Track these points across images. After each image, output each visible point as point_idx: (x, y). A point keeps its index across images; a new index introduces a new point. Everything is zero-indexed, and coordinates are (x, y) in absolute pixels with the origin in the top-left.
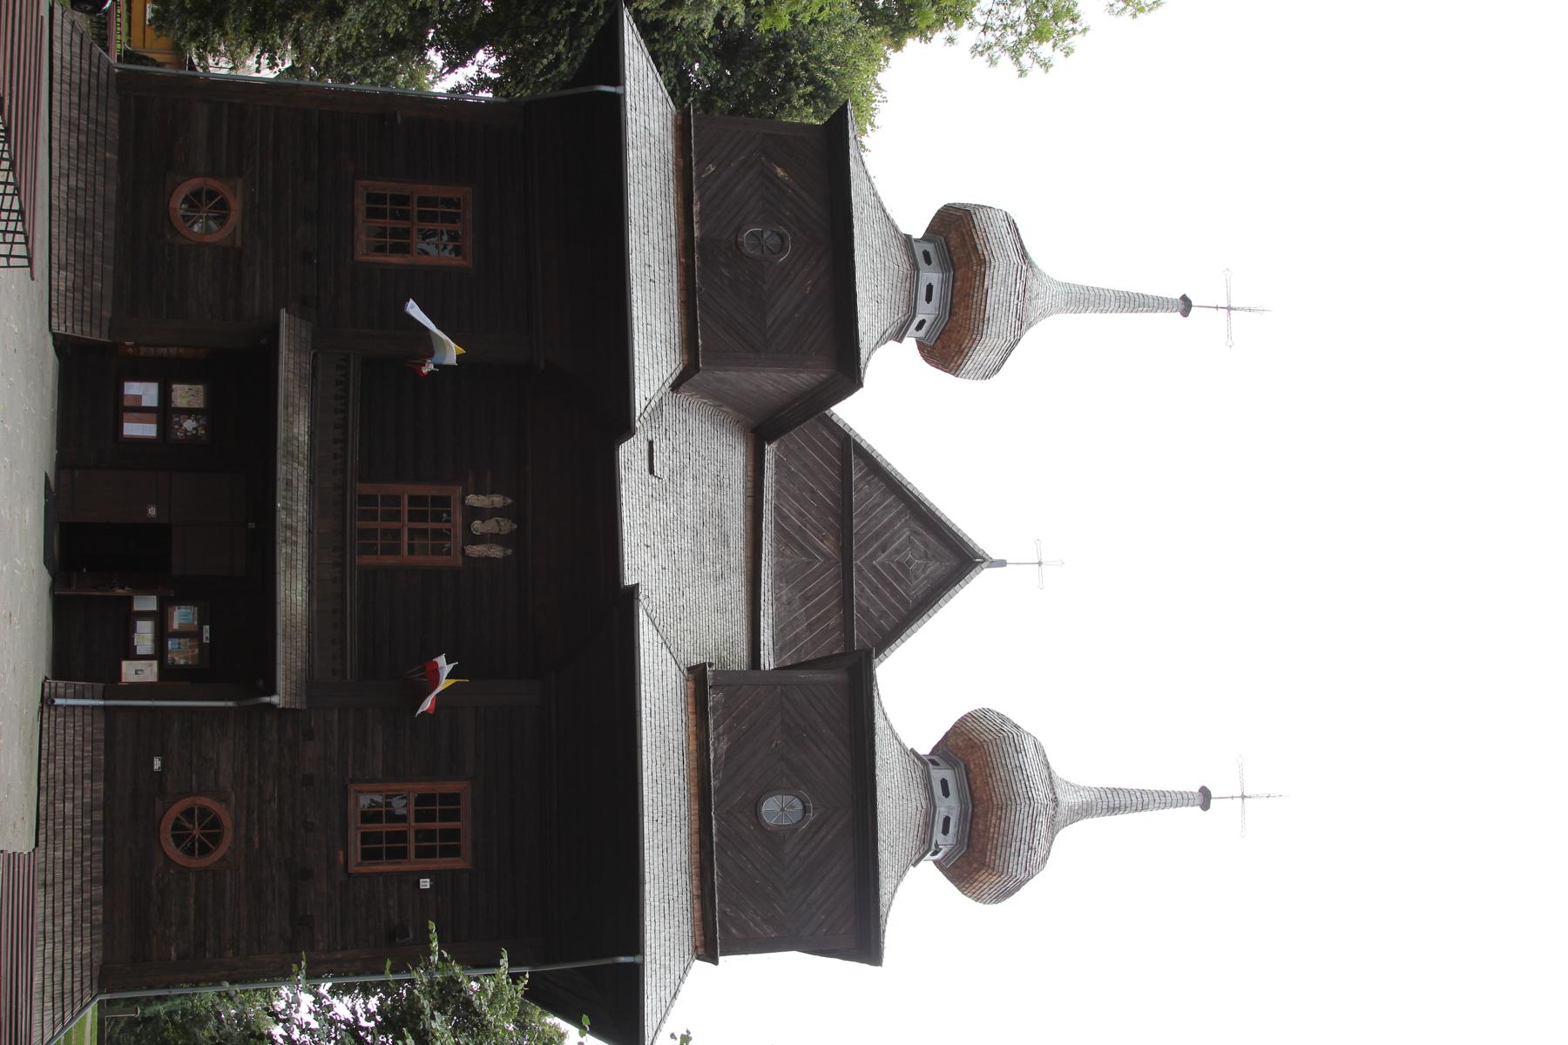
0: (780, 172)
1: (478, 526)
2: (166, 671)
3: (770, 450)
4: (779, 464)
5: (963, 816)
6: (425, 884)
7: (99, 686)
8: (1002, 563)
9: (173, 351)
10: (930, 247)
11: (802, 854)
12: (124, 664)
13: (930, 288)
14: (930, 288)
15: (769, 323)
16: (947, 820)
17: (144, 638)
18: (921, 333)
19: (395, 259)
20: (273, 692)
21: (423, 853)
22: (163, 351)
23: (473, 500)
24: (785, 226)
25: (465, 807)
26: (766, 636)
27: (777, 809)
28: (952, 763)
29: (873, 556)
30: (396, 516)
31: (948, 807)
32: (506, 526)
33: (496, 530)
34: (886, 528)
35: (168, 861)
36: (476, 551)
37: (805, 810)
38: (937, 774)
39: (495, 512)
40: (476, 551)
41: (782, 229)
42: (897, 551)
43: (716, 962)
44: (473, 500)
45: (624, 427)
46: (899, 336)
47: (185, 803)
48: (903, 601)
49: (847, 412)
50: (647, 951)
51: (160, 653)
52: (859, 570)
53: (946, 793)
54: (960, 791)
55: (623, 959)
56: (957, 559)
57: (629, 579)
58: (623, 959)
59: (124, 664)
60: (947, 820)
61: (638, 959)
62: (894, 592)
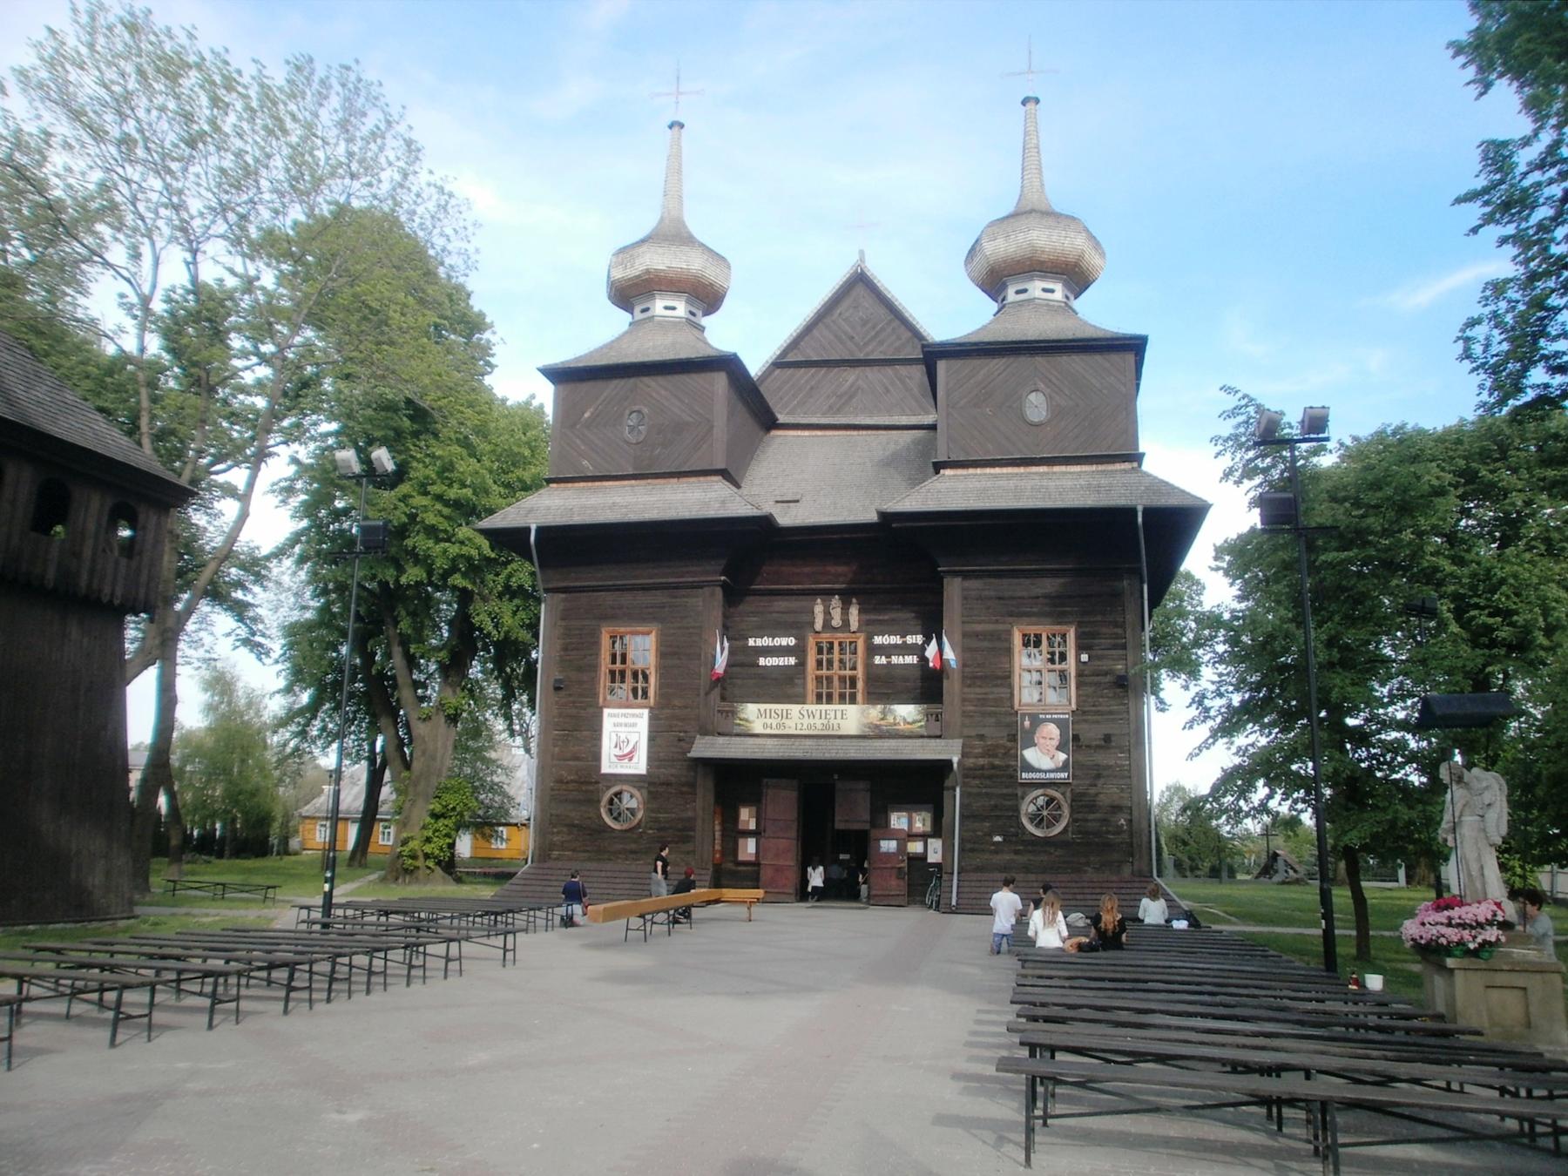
1: (837, 621)
2: (937, 831)
4: (791, 413)
5: (1042, 278)
6: (1085, 658)
7: (945, 877)
8: (862, 253)
9: (717, 828)
10: (637, 310)
12: (930, 860)
13: (666, 308)
14: (666, 308)
16: (1045, 290)
17: (916, 847)
18: (699, 313)
19: (652, 680)
20: (950, 762)
21: (1063, 657)
22: (718, 834)
23: (818, 626)
25: (1032, 630)
26: (913, 420)
27: (1036, 406)
28: (1004, 287)
29: (857, 345)
30: (829, 679)
31: (1036, 288)
32: (836, 601)
33: (839, 610)
35: (1065, 830)
36: (854, 625)
39: (827, 613)
40: (854, 625)
44: (818, 626)
45: (766, 522)
46: (702, 329)
47: (1025, 821)
48: (890, 322)
49: (755, 364)
51: (924, 837)
53: (1025, 291)
55: (1140, 519)
56: (860, 283)
57: (873, 517)
58: (1140, 519)
59: (930, 860)
60: (1045, 290)
61: (1140, 509)
62: (883, 329)
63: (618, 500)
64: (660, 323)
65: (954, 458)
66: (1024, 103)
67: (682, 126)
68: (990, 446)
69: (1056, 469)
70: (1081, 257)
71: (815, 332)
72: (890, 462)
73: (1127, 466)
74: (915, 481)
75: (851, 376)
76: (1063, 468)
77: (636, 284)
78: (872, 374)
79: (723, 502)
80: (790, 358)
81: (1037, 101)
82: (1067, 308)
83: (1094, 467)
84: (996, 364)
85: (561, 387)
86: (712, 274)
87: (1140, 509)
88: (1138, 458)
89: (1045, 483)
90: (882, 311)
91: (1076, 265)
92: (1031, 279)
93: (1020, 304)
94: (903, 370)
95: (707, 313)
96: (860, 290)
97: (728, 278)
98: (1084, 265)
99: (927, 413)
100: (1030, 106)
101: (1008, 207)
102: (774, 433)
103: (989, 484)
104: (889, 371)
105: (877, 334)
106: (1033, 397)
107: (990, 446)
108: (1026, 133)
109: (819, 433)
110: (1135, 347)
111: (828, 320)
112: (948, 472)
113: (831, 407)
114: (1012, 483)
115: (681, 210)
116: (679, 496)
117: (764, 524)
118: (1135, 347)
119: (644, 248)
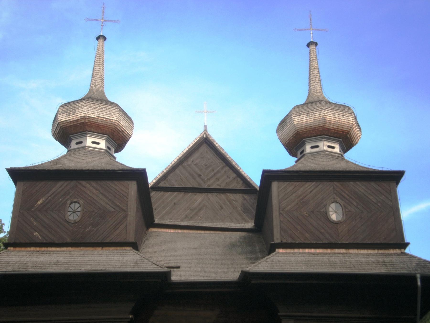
0: (40, 202)
3: (157, 221)
5: (328, 139)
8: (205, 126)
10: (73, 143)
11: (355, 204)
13: (94, 143)
14: (94, 143)
15: (113, 210)
16: (329, 147)
18: (113, 150)
24: (67, 201)
26: (238, 226)
28: (303, 144)
29: (203, 180)
31: (324, 145)
34: (190, 174)
37: (335, 202)
38: (308, 149)
41: (69, 202)
42: (201, 170)
43: (408, 244)
46: (115, 158)
50: (413, 272)
52: (209, 185)
53: (317, 147)
54: (317, 141)
55: (419, 283)
58: (419, 283)
60: (329, 147)
61: (418, 276)
62: (218, 172)
63: (61, 259)
64: (89, 151)
65: (284, 241)
66: (308, 45)
67: (105, 38)
68: (308, 235)
69: (351, 251)
70: (351, 128)
71: (177, 171)
72: (232, 247)
73: (398, 251)
74: (255, 259)
75: (199, 198)
76: (355, 251)
77: (75, 126)
78: (213, 197)
79: (136, 263)
80: (162, 185)
81: (316, 44)
82: (340, 157)
83: (376, 251)
84: (309, 186)
85: (21, 184)
86: (123, 124)
87: (418, 276)
88: (405, 245)
89: (347, 259)
90: (218, 162)
91: (348, 132)
92: (321, 140)
93: (315, 154)
94: (232, 196)
95: (117, 151)
96: (204, 148)
97: (132, 128)
98: (352, 133)
99: (246, 222)
100: (312, 47)
101: (303, 102)
102: (152, 230)
103: (311, 258)
104: (223, 196)
105: (215, 174)
106: (333, 205)
107: (308, 235)
108: (310, 61)
109: (180, 231)
110: (396, 177)
111: (185, 164)
112: (281, 251)
113: (186, 216)
114: (325, 258)
115: (103, 87)
116: (105, 258)
117: (162, 278)
118: (396, 177)
119: (83, 103)
